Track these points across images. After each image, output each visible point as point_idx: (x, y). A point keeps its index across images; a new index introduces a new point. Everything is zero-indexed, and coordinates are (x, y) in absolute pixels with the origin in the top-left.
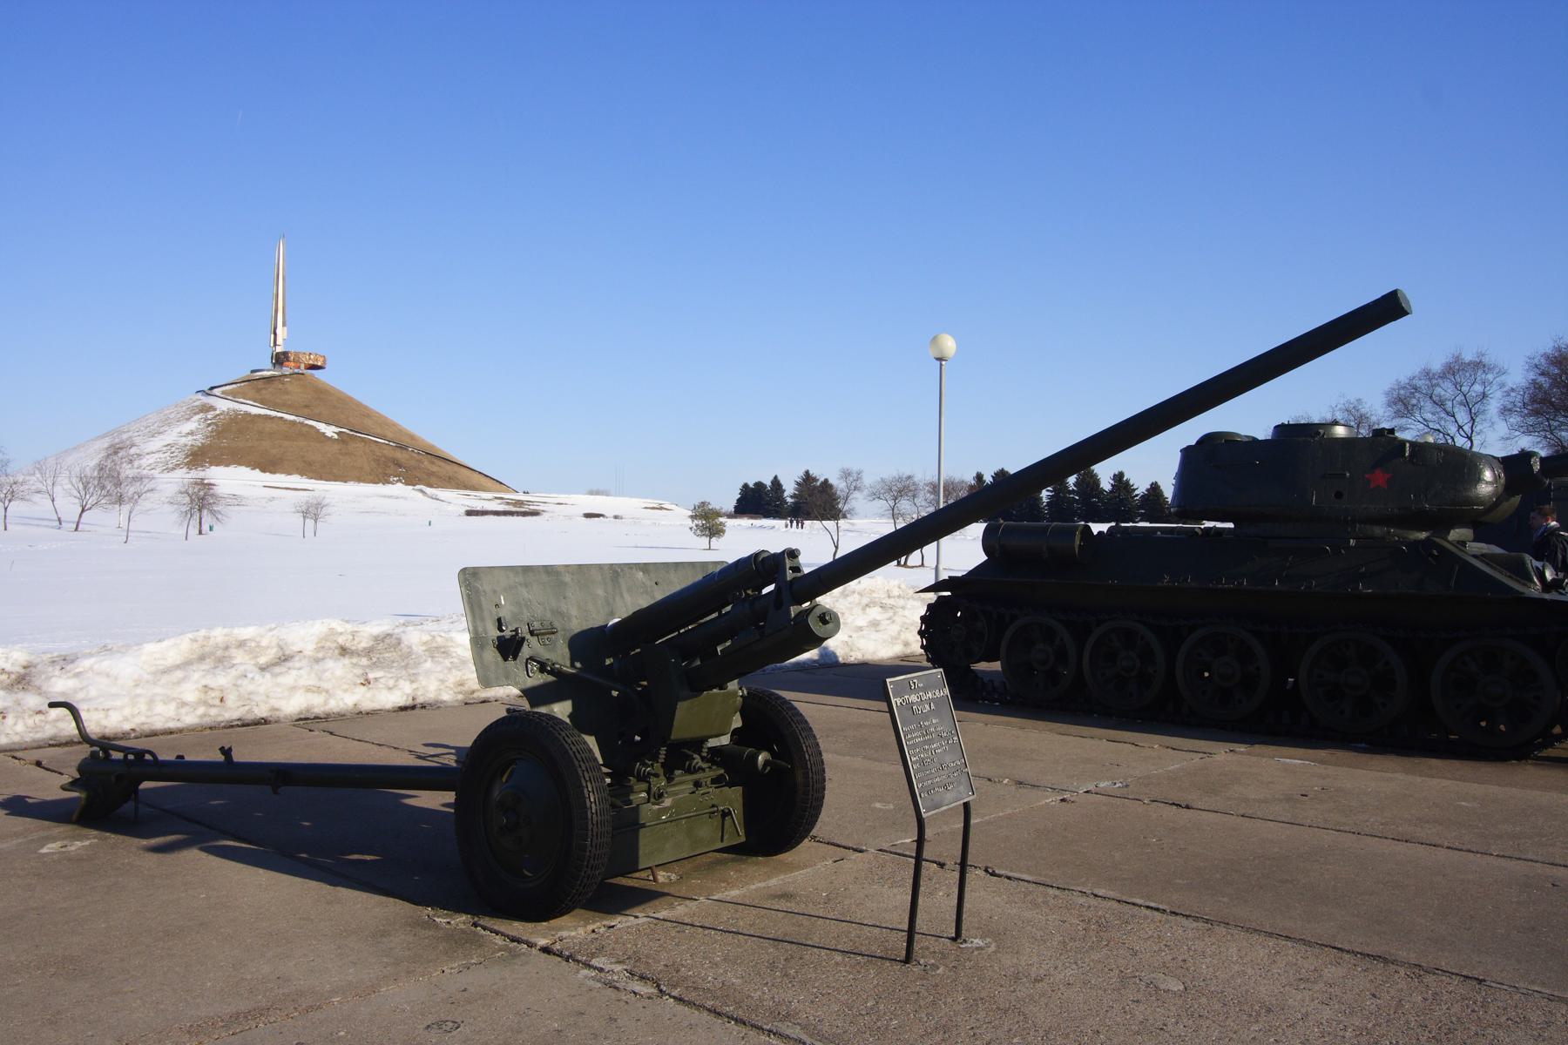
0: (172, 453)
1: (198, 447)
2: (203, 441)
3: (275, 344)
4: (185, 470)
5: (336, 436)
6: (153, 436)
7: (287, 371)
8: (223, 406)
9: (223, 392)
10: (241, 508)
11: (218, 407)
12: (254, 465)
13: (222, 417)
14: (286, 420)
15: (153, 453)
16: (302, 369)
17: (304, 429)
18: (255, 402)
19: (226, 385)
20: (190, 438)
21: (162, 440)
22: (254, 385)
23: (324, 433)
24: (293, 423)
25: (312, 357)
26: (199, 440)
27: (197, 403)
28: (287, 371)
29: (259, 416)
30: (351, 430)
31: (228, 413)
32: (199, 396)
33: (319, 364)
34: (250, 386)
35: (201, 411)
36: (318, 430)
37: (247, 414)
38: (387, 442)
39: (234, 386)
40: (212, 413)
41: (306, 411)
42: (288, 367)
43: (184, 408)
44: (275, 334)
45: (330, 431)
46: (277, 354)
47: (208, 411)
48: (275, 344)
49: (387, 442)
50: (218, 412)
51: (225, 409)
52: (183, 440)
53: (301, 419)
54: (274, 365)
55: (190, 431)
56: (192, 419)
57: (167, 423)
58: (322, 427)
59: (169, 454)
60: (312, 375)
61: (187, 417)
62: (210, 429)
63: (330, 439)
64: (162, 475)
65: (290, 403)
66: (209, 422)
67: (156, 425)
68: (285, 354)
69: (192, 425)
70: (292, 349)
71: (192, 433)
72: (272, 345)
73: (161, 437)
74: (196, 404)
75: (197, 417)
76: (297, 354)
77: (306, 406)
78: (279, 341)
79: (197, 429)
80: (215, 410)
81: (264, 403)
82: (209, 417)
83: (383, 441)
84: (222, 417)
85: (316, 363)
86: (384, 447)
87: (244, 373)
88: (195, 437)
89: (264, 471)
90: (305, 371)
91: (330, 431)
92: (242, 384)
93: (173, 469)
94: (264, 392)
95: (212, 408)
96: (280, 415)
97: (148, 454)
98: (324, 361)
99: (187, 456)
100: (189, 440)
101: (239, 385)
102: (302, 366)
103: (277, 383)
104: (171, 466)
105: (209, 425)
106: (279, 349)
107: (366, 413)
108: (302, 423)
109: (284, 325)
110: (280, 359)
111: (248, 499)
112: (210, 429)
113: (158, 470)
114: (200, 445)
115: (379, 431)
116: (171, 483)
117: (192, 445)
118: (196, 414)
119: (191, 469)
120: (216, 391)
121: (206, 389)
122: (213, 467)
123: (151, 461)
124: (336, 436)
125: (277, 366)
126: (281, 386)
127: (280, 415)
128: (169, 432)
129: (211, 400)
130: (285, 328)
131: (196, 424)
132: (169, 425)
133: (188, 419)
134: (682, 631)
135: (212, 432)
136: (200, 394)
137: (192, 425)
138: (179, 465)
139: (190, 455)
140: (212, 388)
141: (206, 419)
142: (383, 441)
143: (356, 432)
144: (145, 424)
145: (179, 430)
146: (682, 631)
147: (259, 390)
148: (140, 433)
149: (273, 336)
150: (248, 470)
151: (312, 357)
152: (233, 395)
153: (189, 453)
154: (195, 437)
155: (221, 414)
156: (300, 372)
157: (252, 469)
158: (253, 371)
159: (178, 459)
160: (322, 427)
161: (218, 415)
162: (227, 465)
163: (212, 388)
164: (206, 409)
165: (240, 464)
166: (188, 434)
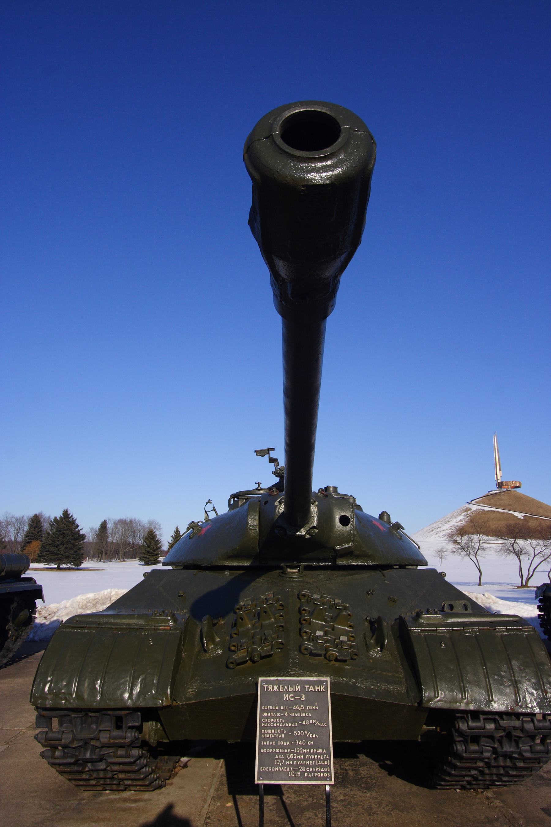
2: (465, 524)
3: (497, 479)
5: (523, 518)
6: (446, 523)
7: (503, 490)
8: (474, 508)
9: (476, 502)
11: (472, 509)
13: (473, 513)
14: (500, 512)
15: (445, 530)
16: (510, 489)
17: (508, 516)
19: (477, 499)
20: (460, 523)
22: (489, 498)
23: (517, 517)
24: (503, 513)
25: (513, 482)
28: (503, 490)
29: (489, 511)
30: (531, 515)
33: (517, 485)
36: (514, 516)
37: (484, 511)
38: (549, 519)
39: (480, 499)
40: (470, 511)
41: (510, 507)
42: (505, 488)
44: (497, 474)
45: (520, 515)
46: (498, 483)
47: (468, 511)
48: (497, 479)
49: (549, 519)
50: (472, 511)
51: (475, 509)
52: (457, 524)
53: (507, 511)
54: (498, 488)
55: (459, 520)
57: (453, 517)
58: (516, 514)
60: (516, 491)
62: (468, 518)
63: (520, 519)
65: (502, 504)
66: (468, 515)
68: (502, 483)
69: (461, 518)
70: (504, 480)
71: (461, 521)
72: (496, 479)
73: (449, 523)
74: (465, 508)
75: (464, 514)
76: (506, 482)
77: (510, 505)
78: (499, 477)
79: (463, 518)
80: (471, 510)
81: (491, 505)
82: (468, 513)
83: (547, 519)
84: (473, 513)
85: (516, 485)
86: (547, 521)
87: (485, 493)
90: (511, 489)
91: (520, 515)
94: (492, 500)
95: (470, 509)
96: (497, 510)
97: (443, 531)
98: (520, 483)
100: (459, 524)
102: (510, 487)
103: (497, 496)
105: (468, 517)
106: (499, 481)
107: (539, 505)
108: (507, 513)
109: (500, 470)
110: (500, 485)
112: (468, 518)
115: (545, 514)
118: (463, 512)
120: (473, 502)
121: (469, 501)
123: (444, 534)
124: (523, 518)
125: (499, 488)
126: (499, 497)
127: (497, 510)
130: (501, 471)
131: (463, 517)
133: (460, 515)
134: (314, 621)
135: (468, 520)
137: (461, 518)
140: (472, 501)
141: (467, 514)
142: (547, 519)
143: (533, 515)
145: (456, 520)
146: (314, 621)
147: (489, 500)
149: (496, 475)
151: (513, 482)
152: (478, 503)
155: (473, 512)
156: (509, 490)
158: (489, 492)
160: (516, 514)
161: (472, 512)
163: (472, 501)
164: (468, 510)
166: (459, 521)
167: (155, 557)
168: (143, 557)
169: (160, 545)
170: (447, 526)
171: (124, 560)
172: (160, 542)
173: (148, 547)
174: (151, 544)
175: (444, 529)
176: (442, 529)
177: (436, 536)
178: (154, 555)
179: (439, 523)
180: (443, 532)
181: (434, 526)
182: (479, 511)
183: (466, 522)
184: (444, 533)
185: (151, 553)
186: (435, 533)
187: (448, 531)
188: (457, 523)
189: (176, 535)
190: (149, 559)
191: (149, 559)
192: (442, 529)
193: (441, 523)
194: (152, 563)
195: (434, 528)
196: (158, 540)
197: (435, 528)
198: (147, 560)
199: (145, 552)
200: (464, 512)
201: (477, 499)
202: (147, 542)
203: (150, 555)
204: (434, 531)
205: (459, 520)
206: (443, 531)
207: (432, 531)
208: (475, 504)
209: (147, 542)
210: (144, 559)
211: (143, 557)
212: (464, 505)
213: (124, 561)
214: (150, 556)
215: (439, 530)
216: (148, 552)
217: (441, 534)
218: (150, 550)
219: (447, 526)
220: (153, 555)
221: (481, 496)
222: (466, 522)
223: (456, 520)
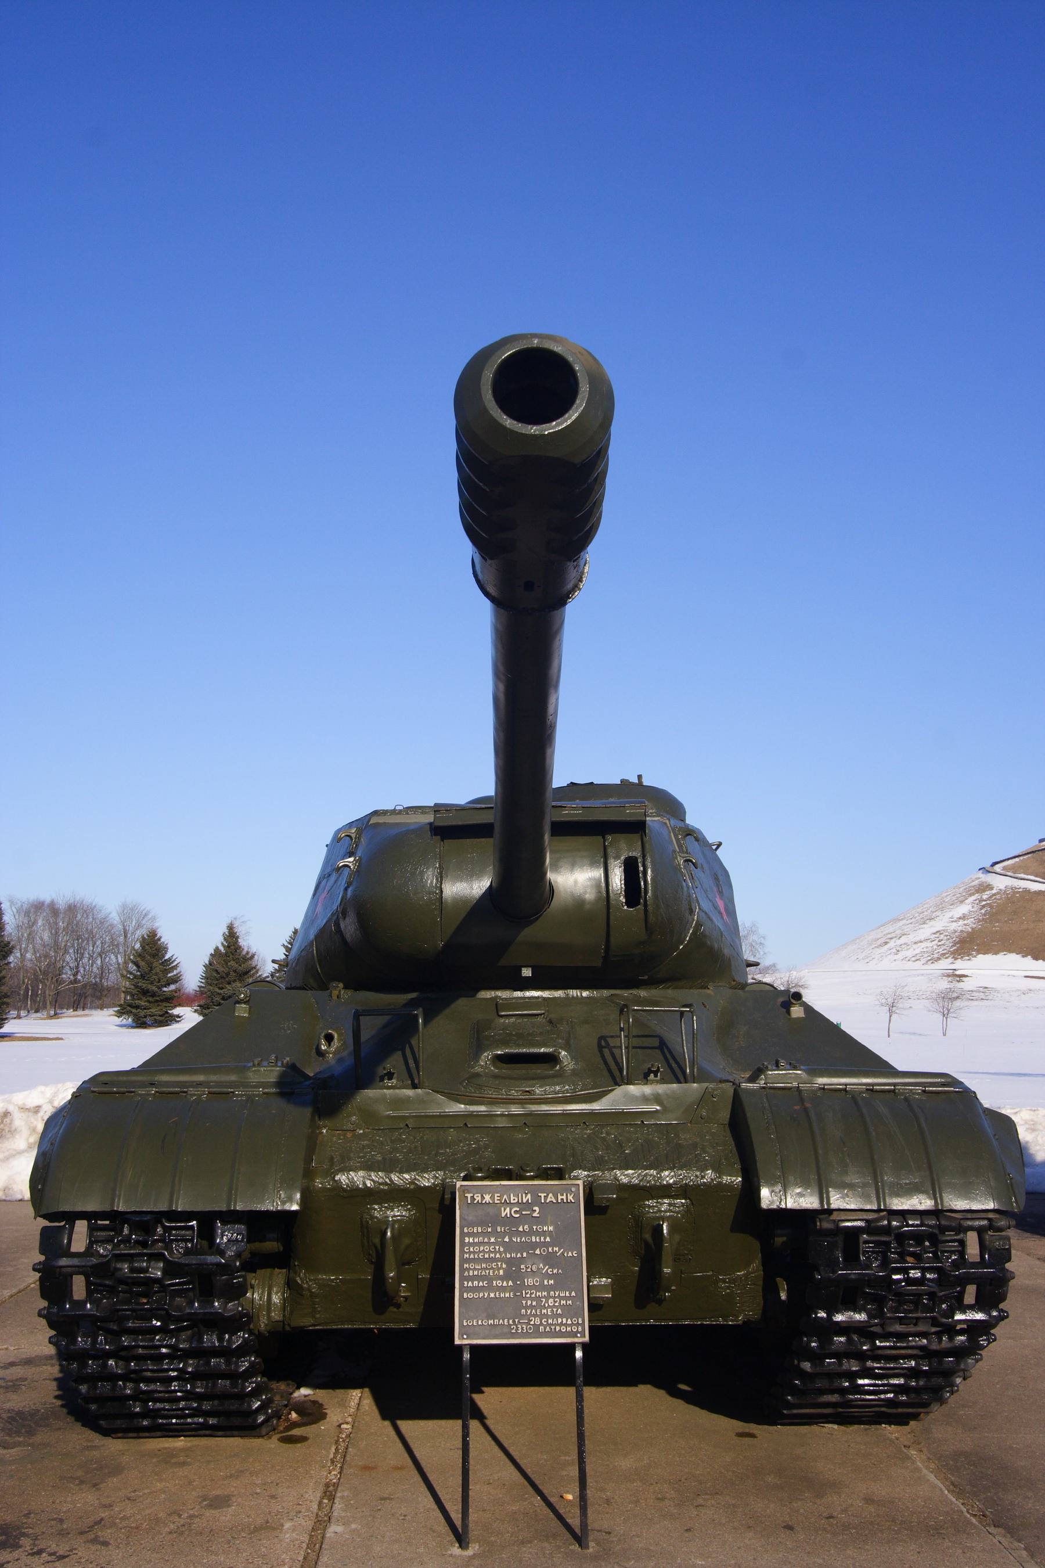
0: (939, 941)
1: (968, 932)
2: (974, 926)
4: (950, 960)
6: (924, 923)
8: (1000, 883)
9: (1004, 868)
10: (985, 1003)
11: (995, 885)
12: (1024, 952)
13: (998, 897)
15: (921, 942)
18: (1036, 876)
19: (1008, 859)
20: (961, 922)
21: (932, 926)
26: (970, 924)
27: (976, 882)
31: (1005, 891)
32: (980, 875)
34: (1033, 857)
35: (977, 891)
37: (1026, 891)
39: (1017, 860)
43: (961, 889)
50: (994, 891)
51: (1002, 887)
52: (954, 926)
56: (966, 901)
57: (941, 907)
59: (936, 942)
61: (960, 899)
62: (983, 911)
64: (926, 967)
66: (984, 903)
67: (929, 911)
69: (964, 909)
71: (963, 917)
73: (932, 923)
74: (974, 883)
80: (992, 889)
82: (985, 897)
84: (998, 897)
88: (965, 922)
89: (1036, 958)
92: (1026, 857)
93: (939, 959)
95: (989, 887)
97: (916, 943)
99: (955, 944)
100: (959, 926)
101: (1021, 858)
104: (936, 956)
105: (983, 906)
111: (998, 992)
112: (983, 911)
113: (923, 961)
114: (970, 930)
116: (922, 975)
117: (962, 931)
118: (971, 895)
119: (956, 959)
120: (998, 868)
121: (987, 865)
122: (980, 956)
123: (917, 951)
128: (941, 917)
129: (991, 879)
131: (970, 906)
132: (942, 909)
133: (962, 902)
135: (985, 915)
136: (981, 871)
137: (964, 909)
138: (943, 955)
139: (957, 943)
141: (981, 900)
144: (920, 910)
148: (913, 920)
150: (1019, 957)
152: (1013, 871)
153: (958, 940)
154: (965, 922)
157: (1023, 956)
159: (945, 947)
161: (994, 895)
162: (996, 953)
165: (1010, 951)
166: (960, 918)
167: (164, 1004)
168: (130, 1006)
169: (175, 972)
170: (926, 931)
171: (56, 1014)
172: (176, 967)
173: (142, 977)
174: (151, 969)
175: (917, 939)
176: (912, 938)
177: (896, 957)
178: (162, 1001)
179: (904, 922)
180: (915, 946)
181: (891, 930)
182: (1015, 893)
183: (979, 921)
184: (918, 949)
185: (153, 995)
186: (894, 950)
187: (929, 944)
188: (954, 924)
189: (229, 947)
190: (148, 1012)
191: (148, 1012)
192: (912, 938)
193: (912, 921)
194: (156, 1021)
195: (889, 936)
196: (170, 959)
197: (893, 935)
198: (142, 1013)
199: (134, 992)
200: (973, 894)
201: (1008, 859)
202: (142, 964)
203: (151, 999)
204: (891, 944)
205: (960, 915)
206: (916, 943)
207: (886, 943)
208: (1002, 872)
209: (142, 964)
210: (134, 1011)
211: (130, 1006)
212: (974, 877)
213: (56, 1016)
214: (149, 1001)
215: (903, 940)
216: (145, 992)
217: (909, 953)
218: (150, 986)
219: (926, 931)
220: (157, 1001)
221: (1016, 854)
222: (979, 921)
223: (950, 914)
